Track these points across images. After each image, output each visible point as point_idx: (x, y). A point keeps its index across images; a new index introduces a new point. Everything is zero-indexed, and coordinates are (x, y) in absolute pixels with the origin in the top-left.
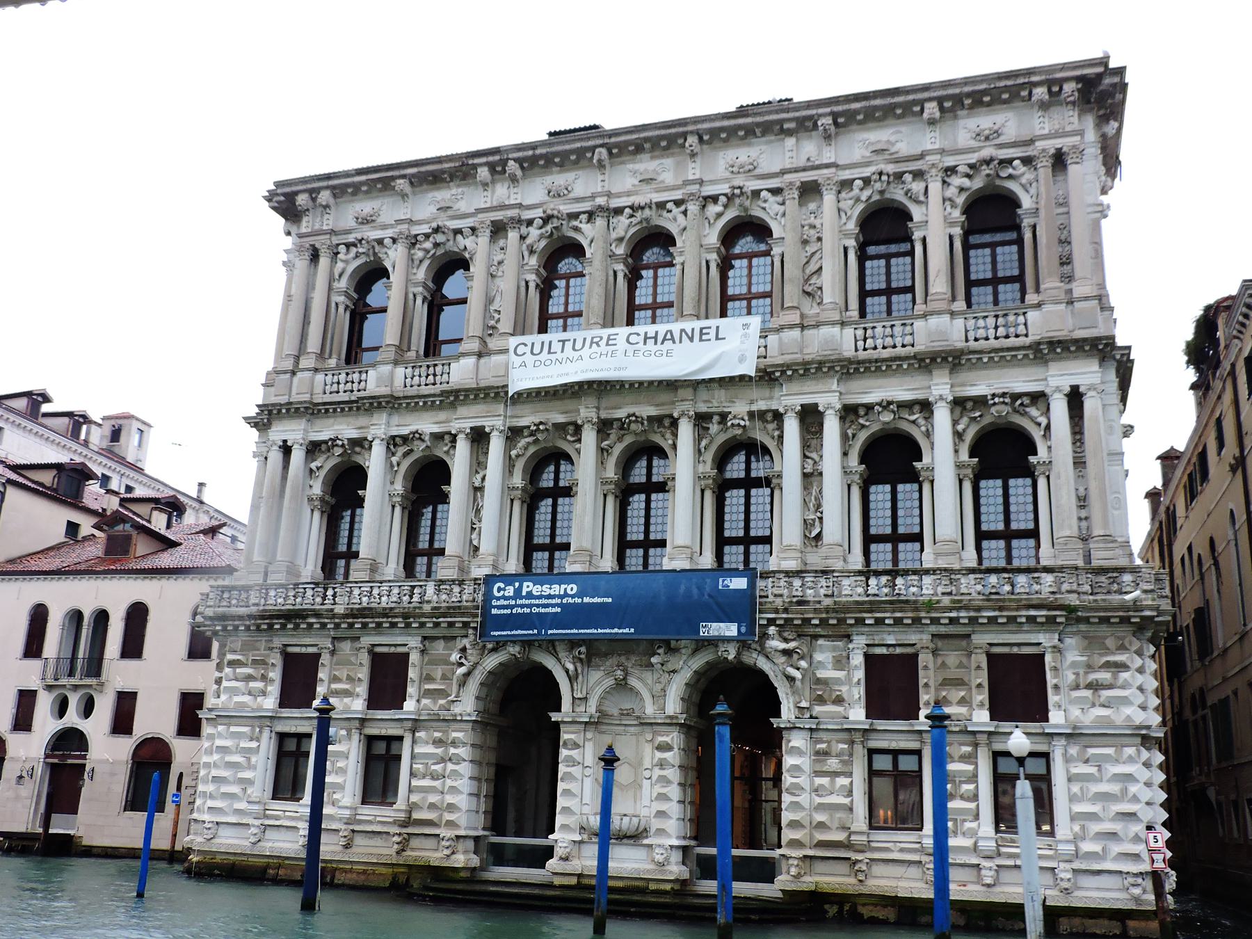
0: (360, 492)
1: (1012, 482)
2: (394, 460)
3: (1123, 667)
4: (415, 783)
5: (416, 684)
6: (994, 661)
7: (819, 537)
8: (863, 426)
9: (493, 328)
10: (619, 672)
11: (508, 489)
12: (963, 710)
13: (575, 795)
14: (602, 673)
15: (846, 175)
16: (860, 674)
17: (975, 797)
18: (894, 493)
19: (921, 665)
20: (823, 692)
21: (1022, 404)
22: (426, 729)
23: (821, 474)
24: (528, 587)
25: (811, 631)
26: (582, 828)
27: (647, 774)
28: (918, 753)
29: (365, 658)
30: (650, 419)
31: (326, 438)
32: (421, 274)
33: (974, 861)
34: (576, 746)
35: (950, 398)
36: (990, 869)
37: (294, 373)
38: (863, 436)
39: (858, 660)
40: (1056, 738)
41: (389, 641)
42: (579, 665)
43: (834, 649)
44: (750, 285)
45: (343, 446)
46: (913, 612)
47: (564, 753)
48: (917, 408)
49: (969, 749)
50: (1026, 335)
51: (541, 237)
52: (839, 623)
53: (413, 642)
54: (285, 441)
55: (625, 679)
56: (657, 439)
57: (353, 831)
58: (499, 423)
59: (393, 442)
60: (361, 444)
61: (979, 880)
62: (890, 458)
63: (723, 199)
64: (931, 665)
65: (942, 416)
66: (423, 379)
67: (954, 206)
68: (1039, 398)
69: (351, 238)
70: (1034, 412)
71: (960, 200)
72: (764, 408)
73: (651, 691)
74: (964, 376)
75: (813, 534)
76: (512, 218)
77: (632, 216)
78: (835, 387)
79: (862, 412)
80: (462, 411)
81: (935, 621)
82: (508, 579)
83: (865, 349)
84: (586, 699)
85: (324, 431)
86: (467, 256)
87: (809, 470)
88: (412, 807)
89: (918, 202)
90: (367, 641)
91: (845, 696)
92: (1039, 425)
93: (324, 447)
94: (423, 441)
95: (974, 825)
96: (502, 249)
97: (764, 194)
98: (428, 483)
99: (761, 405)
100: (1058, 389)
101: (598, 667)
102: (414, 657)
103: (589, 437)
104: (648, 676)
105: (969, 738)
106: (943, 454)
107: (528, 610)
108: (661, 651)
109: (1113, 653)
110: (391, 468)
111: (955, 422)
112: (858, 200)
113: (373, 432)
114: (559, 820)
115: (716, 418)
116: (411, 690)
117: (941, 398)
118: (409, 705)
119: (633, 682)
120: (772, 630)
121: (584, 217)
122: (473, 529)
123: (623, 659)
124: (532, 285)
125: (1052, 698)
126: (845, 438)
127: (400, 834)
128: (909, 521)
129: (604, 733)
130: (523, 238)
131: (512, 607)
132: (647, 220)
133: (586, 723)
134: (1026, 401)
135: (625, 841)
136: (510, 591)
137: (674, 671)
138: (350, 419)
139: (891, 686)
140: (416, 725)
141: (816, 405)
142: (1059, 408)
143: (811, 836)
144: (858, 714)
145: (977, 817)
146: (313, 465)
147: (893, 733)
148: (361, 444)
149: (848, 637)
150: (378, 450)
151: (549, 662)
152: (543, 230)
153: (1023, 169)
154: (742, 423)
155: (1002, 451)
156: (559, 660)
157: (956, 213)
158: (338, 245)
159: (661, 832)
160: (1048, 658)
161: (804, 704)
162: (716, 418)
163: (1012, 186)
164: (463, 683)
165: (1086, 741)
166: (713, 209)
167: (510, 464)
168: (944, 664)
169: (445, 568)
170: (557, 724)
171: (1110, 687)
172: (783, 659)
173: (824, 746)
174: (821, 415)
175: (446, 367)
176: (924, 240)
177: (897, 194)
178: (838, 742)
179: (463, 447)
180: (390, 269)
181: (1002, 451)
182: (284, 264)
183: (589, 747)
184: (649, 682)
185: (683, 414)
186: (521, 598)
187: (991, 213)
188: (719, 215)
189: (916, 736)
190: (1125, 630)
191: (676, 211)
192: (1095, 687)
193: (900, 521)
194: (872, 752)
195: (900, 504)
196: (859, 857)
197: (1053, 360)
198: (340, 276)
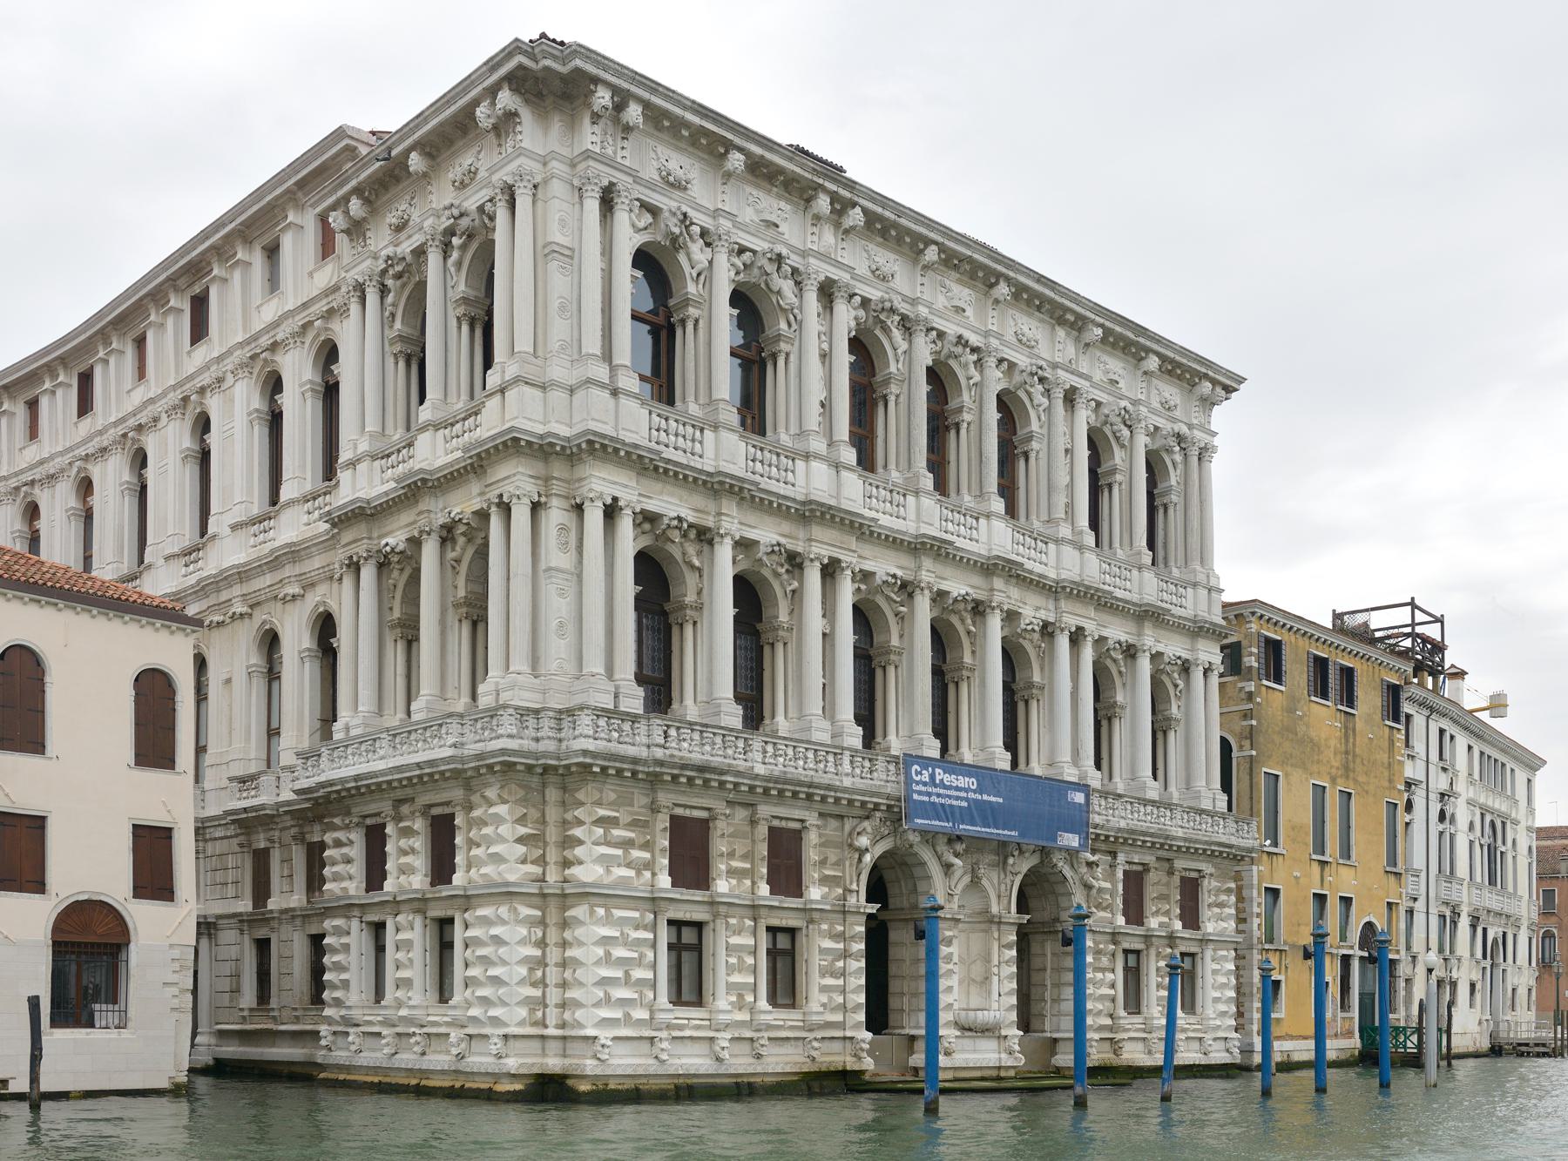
24: (940, 774)
53: (812, 819)
80: (817, 531)
82: (926, 762)
104: (994, 875)
107: (926, 799)
131: (929, 794)
136: (926, 777)
151: (926, 855)
186: (936, 786)
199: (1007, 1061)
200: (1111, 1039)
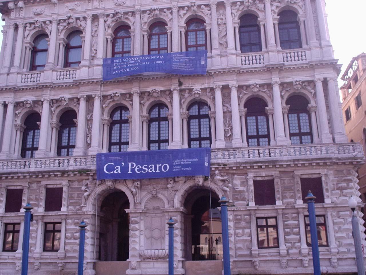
0: (38, 123)
1: (301, 115)
2: (53, 109)
3: (351, 181)
4: (67, 241)
5: (66, 200)
6: (303, 181)
7: (231, 136)
8: (245, 94)
9: (94, 56)
10: (154, 192)
11: (102, 120)
12: (293, 200)
13: (137, 243)
14: (146, 192)
16: (252, 188)
17: (299, 234)
18: (257, 119)
19: (275, 183)
21: (305, 85)
22: (71, 219)
23: (231, 112)
25: (231, 172)
29: (44, 191)
30: (161, 91)
31: (23, 100)
32: (62, 36)
33: (300, 258)
34: (136, 222)
35: (280, 83)
36: (307, 260)
37: (8, 74)
38: (245, 98)
39: (251, 182)
40: (328, 209)
41: (53, 183)
42: (137, 189)
45: (30, 104)
46: (273, 163)
47: (132, 226)
48: (266, 86)
49: (296, 215)
50: (306, 60)
51: (113, 21)
52: (242, 169)
54: (5, 102)
55: (156, 194)
56: (163, 100)
57: (40, 263)
58: (98, 93)
59: (52, 102)
60: (39, 103)
61: (303, 266)
63: (186, 8)
64: (279, 183)
65: (277, 90)
66: (65, 76)
67: (274, 13)
68: (312, 83)
69: (32, 21)
70: (309, 88)
72: (207, 87)
73: (167, 199)
74: (283, 74)
75: (228, 135)
76: (101, 14)
77: (150, 14)
78: (235, 78)
79: (245, 88)
80: (82, 89)
81: (281, 166)
83: (245, 64)
84: (140, 203)
85: (23, 98)
86: (82, 28)
87: (225, 110)
88: (66, 251)
90: (44, 183)
91: (247, 197)
92: (311, 93)
93: (21, 104)
94: (66, 101)
95: (299, 244)
96: (96, 26)
97: (203, 6)
98: (67, 119)
99: (206, 86)
100: (319, 79)
101: (144, 190)
102: (65, 189)
103: (136, 99)
104: (166, 193)
105: (295, 211)
108: (172, 182)
109: (347, 177)
110: (51, 113)
111: (281, 92)
112: (238, 10)
113: (44, 98)
114: (131, 253)
115: (187, 91)
116: (64, 202)
117: (276, 82)
118: (64, 209)
119: (160, 195)
120: (217, 172)
121: (130, 14)
122: (87, 137)
123: (155, 186)
124: (109, 40)
125: (326, 194)
126: (239, 98)
127: (61, 263)
128: (263, 130)
129: (147, 217)
130: (105, 22)
132: (156, 15)
133: (141, 213)
134: (306, 84)
135: (159, 260)
137: (177, 190)
138: (33, 93)
139: (265, 192)
140: (67, 217)
141: (228, 85)
142: (320, 86)
143: (236, 254)
145: (300, 241)
146: (17, 112)
147: (266, 210)
148: (39, 103)
150: (46, 106)
152: (114, 19)
154: (199, 92)
155: (298, 104)
156: (128, 188)
158: (26, 23)
160: (323, 179)
162: (187, 91)
163: (295, 6)
164: (87, 199)
165: (338, 209)
166: (182, 12)
167: (103, 109)
168: (284, 183)
169: (78, 151)
170: (128, 214)
171: (346, 188)
172: (222, 183)
173: (239, 217)
175: (75, 72)
176: (264, 25)
177: (254, 9)
178: (245, 215)
179: (83, 104)
180: (49, 33)
181: (298, 104)
182: (2, 31)
183: (142, 222)
184: (166, 195)
185: (175, 89)
188: (185, 14)
189: (275, 211)
190: (351, 167)
191: (168, 12)
192: (341, 189)
193: (260, 130)
194: (257, 218)
195: (259, 124)
196: (256, 259)
197: (317, 68)
198: (27, 36)
200: (251, 261)
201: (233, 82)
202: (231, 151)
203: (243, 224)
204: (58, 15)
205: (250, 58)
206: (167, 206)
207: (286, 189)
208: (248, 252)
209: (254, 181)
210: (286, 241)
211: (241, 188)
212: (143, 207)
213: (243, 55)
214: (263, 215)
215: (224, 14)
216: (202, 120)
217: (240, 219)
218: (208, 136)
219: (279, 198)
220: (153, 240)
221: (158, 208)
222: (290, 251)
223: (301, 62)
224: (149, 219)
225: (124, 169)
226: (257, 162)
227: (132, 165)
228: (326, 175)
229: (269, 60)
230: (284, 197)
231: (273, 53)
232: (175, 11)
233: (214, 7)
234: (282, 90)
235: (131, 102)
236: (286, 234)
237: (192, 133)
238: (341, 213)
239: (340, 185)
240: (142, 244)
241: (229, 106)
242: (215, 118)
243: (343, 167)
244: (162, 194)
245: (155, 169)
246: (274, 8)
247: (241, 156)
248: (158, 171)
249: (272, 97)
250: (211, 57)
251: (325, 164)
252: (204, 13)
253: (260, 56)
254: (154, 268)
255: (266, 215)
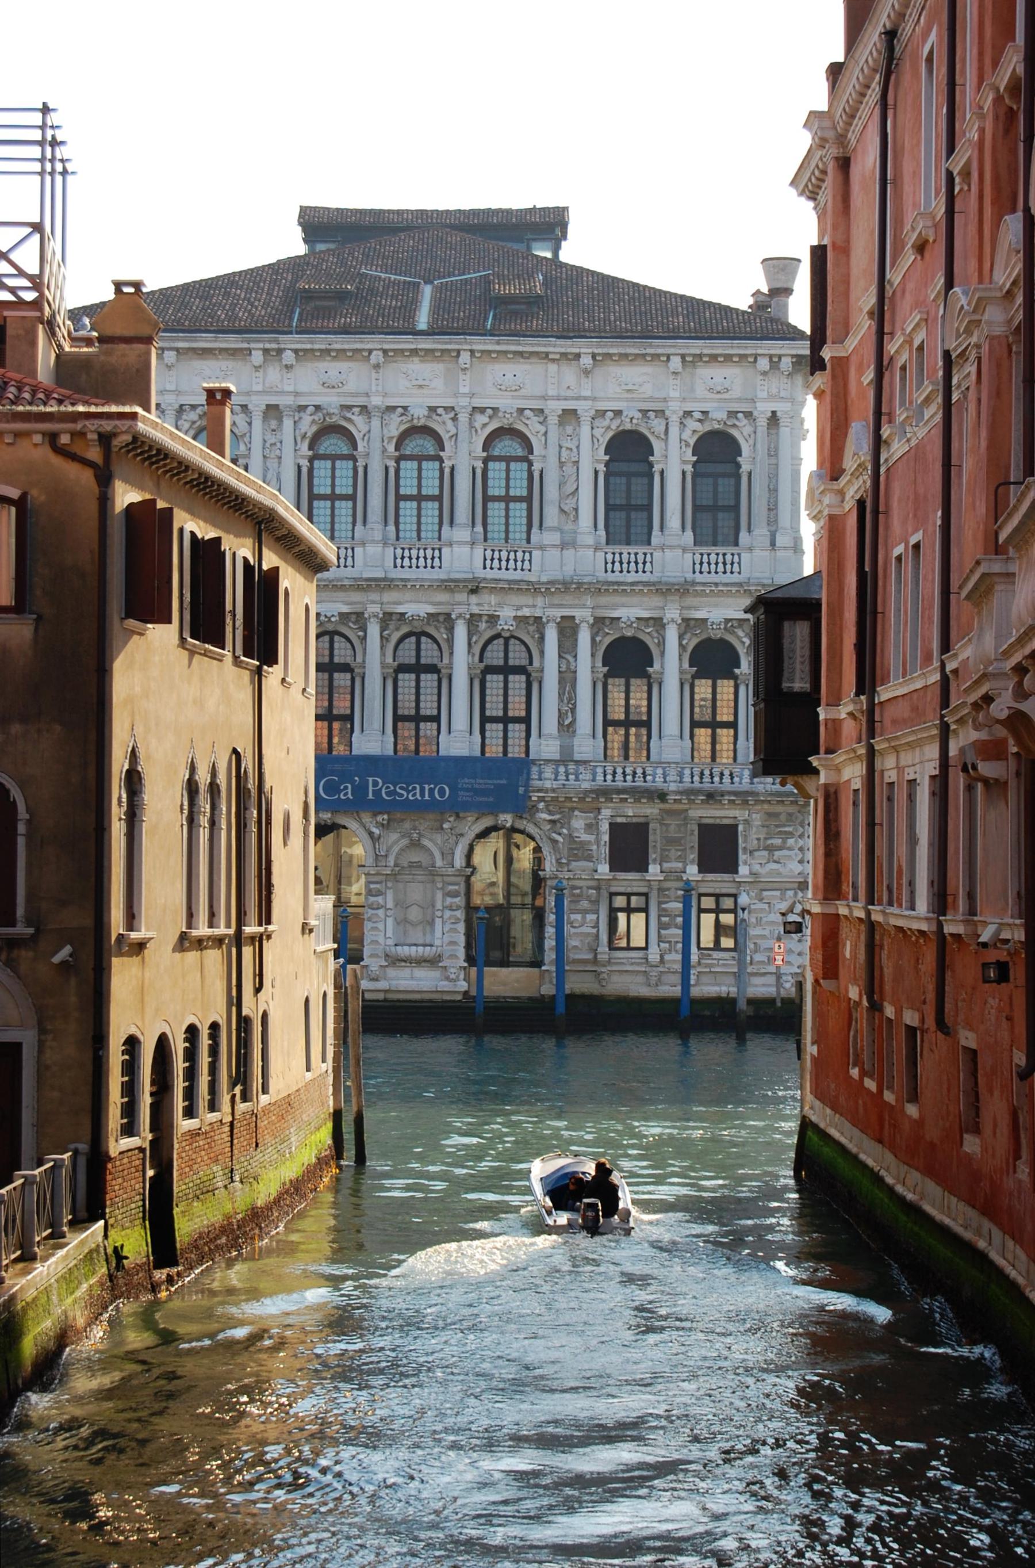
3: (791, 835)
12: (680, 865)
15: (602, 406)
16: (606, 838)
19: (651, 832)
20: (579, 851)
26: (387, 955)
27: (439, 914)
28: (646, 895)
39: (605, 827)
43: (586, 818)
44: (508, 487)
48: (651, 622)
51: (313, 422)
62: (628, 658)
65: (672, 635)
67: (687, 445)
71: (692, 442)
74: (690, 601)
75: (567, 722)
77: (402, 415)
79: (607, 622)
89: (658, 437)
91: (595, 853)
97: (527, 412)
99: (526, 612)
104: (439, 838)
106: (671, 663)
108: (451, 819)
109: (784, 826)
111: (681, 637)
112: (609, 428)
115: (485, 618)
117: (673, 620)
119: (426, 842)
120: (541, 805)
121: (356, 410)
125: (742, 857)
126: (593, 640)
137: (462, 835)
144: (604, 868)
147: (629, 881)
149: (599, 810)
153: (745, 422)
157: (690, 451)
159: (453, 956)
160: (741, 828)
161: (564, 861)
162: (485, 618)
163: (734, 432)
166: (481, 419)
171: (780, 848)
174: (577, 626)
176: (662, 473)
183: (390, 895)
185: (460, 616)
187: (716, 451)
188: (485, 425)
191: (447, 417)
192: (771, 849)
196: (603, 970)
199: (444, 985)
201: (583, 614)
202: (572, 767)
203: (585, 904)
204: (178, 392)
205: (625, 557)
206: (439, 863)
207: (671, 841)
208: (590, 956)
209: (610, 824)
210: (660, 939)
211: (585, 837)
212: (392, 864)
213: (610, 549)
214: (622, 890)
215: (576, 435)
216: (511, 677)
217: (579, 896)
218: (523, 714)
219: (655, 860)
220: (409, 927)
221: (418, 865)
222: (667, 957)
223: (728, 578)
224: (401, 885)
225: (360, 790)
226: (619, 791)
227: (375, 783)
228: (746, 822)
229: (663, 567)
230: (663, 859)
231: (673, 550)
232: (463, 418)
233: (553, 420)
234: (685, 633)
235: (361, 634)
236: (662, 926)
237: (488, 705)
238: (765, 893)
239: (769, 842)
240: (389, 934)
241: (571, 659)
242: (540, 683)
243: (780, 809)
244: (430, 840)
245: (422, 794)
246: (687, 435)
247: (589, 776)
248: (427, 797)
249: (662, 644)
250: (542, 548)
251: (746, 802)
252: (532, 428)
253: (645, 554)
254: (412, 978)
255: (629, 890)
